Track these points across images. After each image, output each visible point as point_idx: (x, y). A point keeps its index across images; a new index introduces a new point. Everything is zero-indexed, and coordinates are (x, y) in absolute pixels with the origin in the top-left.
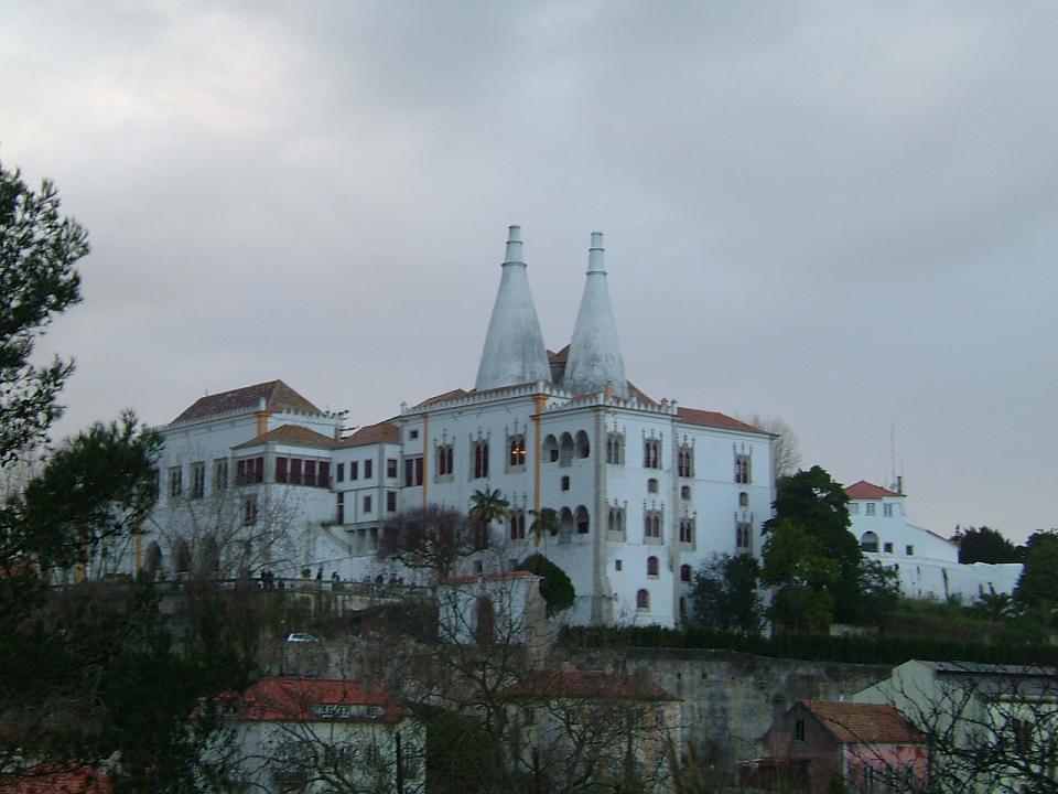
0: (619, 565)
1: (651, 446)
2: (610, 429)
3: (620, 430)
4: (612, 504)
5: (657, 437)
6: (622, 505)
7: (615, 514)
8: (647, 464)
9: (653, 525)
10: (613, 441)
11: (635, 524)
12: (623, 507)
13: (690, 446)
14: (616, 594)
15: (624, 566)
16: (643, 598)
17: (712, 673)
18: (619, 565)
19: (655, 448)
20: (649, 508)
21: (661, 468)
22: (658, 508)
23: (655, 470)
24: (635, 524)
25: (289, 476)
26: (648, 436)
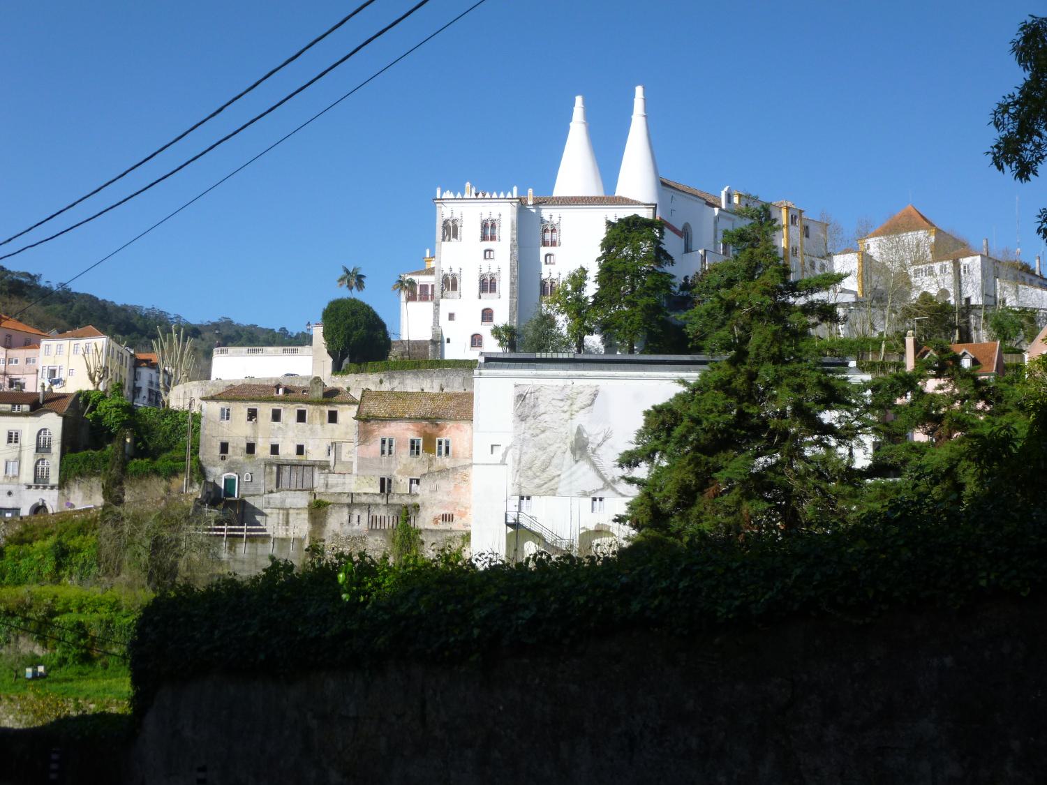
0: (451, 317)
1: (490, 225)
2: (447, 216)
3: (457, 216)
4: (447, 271)
5: (495, 216)
6: (456, 271)
7: (450, 278)
8: (484, 238)
9: (487, 285)
10: (451, 225)
11: (469, 285)
12: (458, 272)
13: (555, 223)
14: (448, 341)
15: (456, 317)
16: (476, 340)
17: (447, 386)
18: (451, 317)
19: (493, 226)
20: (485, 271)
21: (500, 240)
22: (494, 270)
23: (493, 242)
24: (469, 285)
25: (418, 297)
26: (485, 217)
